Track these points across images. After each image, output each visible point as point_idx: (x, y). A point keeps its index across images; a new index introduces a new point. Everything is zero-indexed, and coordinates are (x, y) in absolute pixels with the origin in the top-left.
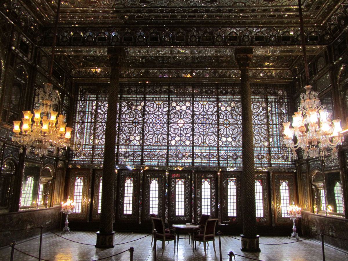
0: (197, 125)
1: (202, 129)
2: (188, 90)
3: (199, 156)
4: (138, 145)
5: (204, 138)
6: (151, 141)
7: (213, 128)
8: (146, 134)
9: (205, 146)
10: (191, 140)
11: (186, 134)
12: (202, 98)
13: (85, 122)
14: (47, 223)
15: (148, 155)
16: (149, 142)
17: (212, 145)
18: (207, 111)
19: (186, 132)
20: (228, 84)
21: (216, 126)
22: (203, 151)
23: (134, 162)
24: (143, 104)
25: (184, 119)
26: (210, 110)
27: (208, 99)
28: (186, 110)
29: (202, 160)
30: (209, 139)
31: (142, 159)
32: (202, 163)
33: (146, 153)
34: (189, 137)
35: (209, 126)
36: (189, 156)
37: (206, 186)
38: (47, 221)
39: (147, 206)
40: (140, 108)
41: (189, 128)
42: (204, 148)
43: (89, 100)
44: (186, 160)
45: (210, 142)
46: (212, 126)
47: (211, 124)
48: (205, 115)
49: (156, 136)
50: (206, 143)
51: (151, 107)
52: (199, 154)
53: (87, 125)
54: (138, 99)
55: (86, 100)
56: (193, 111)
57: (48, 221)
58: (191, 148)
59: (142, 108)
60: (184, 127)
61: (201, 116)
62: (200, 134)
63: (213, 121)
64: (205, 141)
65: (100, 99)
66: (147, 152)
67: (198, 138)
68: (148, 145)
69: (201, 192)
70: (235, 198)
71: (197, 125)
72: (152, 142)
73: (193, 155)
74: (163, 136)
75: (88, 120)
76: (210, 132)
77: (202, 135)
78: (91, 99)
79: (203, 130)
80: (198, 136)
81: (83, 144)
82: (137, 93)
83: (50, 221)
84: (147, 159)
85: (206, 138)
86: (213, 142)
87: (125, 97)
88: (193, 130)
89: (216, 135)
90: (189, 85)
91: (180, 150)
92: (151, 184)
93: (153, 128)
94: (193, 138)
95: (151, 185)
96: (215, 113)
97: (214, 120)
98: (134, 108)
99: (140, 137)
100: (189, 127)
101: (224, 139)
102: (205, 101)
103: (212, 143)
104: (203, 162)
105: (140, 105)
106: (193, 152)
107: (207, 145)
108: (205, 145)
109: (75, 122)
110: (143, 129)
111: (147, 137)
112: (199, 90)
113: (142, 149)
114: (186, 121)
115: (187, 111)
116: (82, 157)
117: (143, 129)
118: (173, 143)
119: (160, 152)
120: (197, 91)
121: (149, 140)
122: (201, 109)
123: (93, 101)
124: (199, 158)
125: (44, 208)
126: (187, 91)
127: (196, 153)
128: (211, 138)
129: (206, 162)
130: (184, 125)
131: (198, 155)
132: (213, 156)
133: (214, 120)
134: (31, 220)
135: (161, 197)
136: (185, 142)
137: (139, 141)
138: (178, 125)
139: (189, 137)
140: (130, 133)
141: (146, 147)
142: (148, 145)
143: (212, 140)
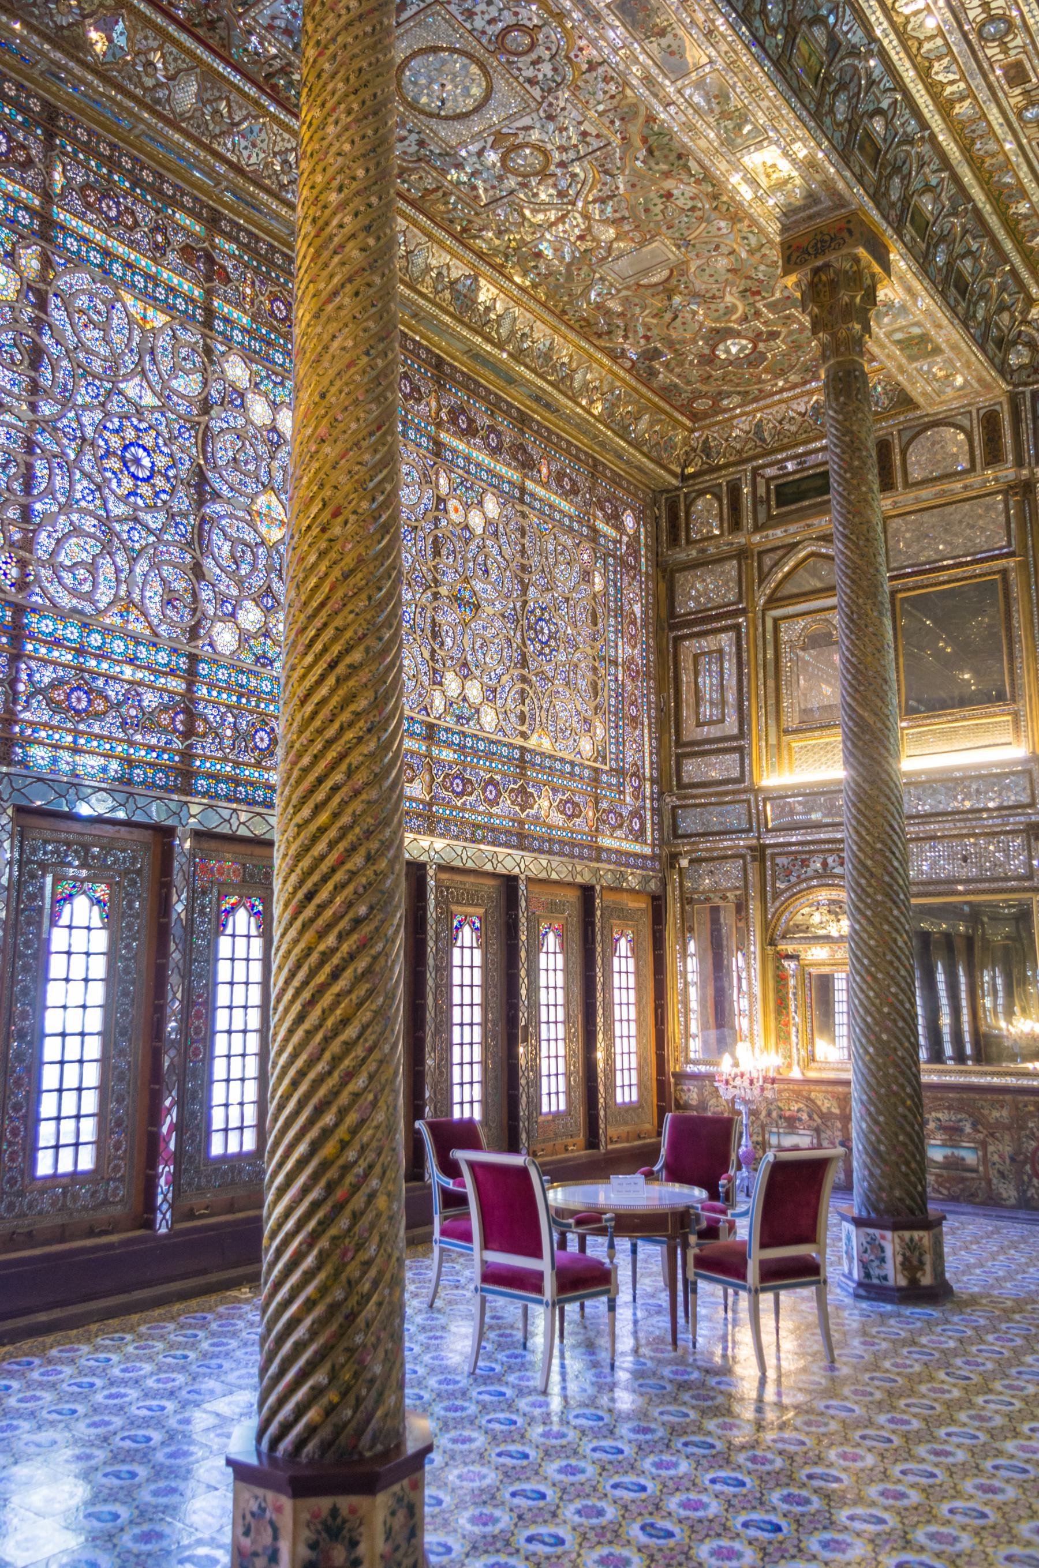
6: (86, 587)
8: (50, 518)
15: (59, 695)
16: (73, 592)
20: (480, 385)
33: (47, 675)
39: (17, 1107)
49: (121, 559)
66: (55, 663)
68: (62, 615)
74: (167, 571)
91: (259, 699)
92: (53, 923)
95: (59, 939)
101: (452, 683)
118: (225, 638)
119: (140, 683)
121: (70, 569)
135: (21, 1035)
138: (251, 525)
141: (47, 626)
142: (62, 615)
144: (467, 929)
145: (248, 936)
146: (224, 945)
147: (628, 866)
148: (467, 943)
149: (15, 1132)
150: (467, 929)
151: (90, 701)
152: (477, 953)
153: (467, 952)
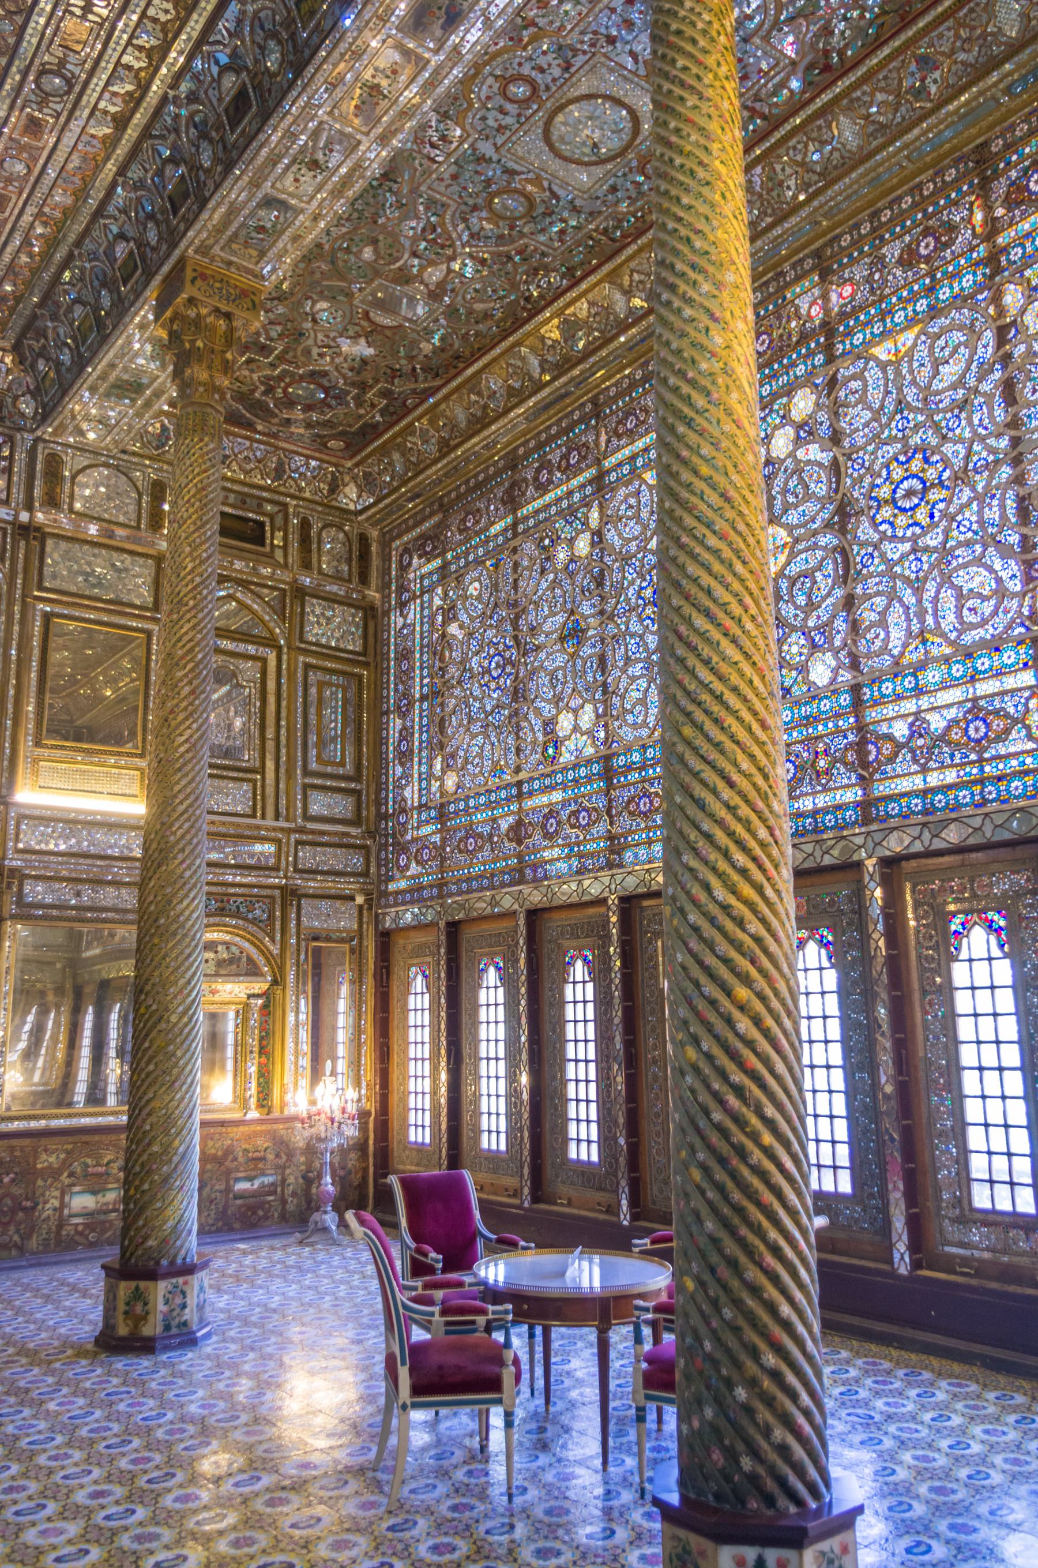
0: (865, 524)
1: (903, 539)
2: (797, 308)
3: (899, 747)
4: (589, 762)
5: (920, 601)
7: (980, 498)
9: (935, 660)
10: (837, 643)
11: (811, 606)
12: (883, 315)
13: (423, 698)
14: (242, 1186)
17: (986, 633)
18: (927, 393)
19: (809, 597)
21: (1006, 472)
22: (925, 702)
23: (581, 856)
24: (595, 515)
25: (793, 517)
26: (950, 372)
27: (922, 305)
28: (792, 455)
29: (924, 770)
30: (960, 596)
31: (611, 837)
32: (925, 792)
34: (830, 623)
35: (948, 501)
36: (835, 761)
37: (981, 970)
38: (237, 1180)
39: (657, 1115)
40: (583, 546)
41: (819, 568)
42: (932, 676)
43: (422, 593)
44: (825, 789)
45: (970, 618)
46: (973, 489)
47: (962, 477)
48: (917, 427)
50: (943, 635)
51: (630, 518)
52: (900, 730)
53: (422, 710)
54: (576, 497)
55: (414, 598)
56: (836, 438)
57: (250, 1179)
58: (845, 699)
59: (593, 544)
60: (794, 569)
61: (891, 450)
62: (894, 577)
63: (976, 447)
64: (930, 620)
65: (453, 568)
67: (883, 614)
69: (952, 1016)
70: (1017, 1063)
71: (865, 524)
72: (645, 724)
73: (860, 747)
75: (422, 686)
76: (960, 544)
77: (907, 581)
78: (426, 582)
79: (907, 546)
80: (880, 602)
81: (413, 808)
82: (569, 470)
83: (268, 1180)
84: (631, 832)
85: (935, 600)
86: (987, 608)
87: (526, 518)
88: (847, 574)
89: (1005, 552)
90: (798, 279)
93: (641, 637)
94: (855, 627)
96: (980, 380)
97: (982, 439)
98: (562, 556)
99: (596, 709)
100: (819, 553)
102: (911, 322)
103: (984, 622)
104: (934, 779)
105: (585, 524)
106: (861, 728)
107: (951, 643)
108: (935, 652)
109: (387, 713)
110: (602, 660)
111: (623, 697)
112: (859, 272)
113: (608, 774)
114: (798, 526)
115: (800, 454)
116: (414, 869)
117: (602, 660)
120: (847, 290)
122: (888, 393)
123: (431, 590)
124: (904, 763)
125: (237, 1116)
126: (789, 321)
127: (884, 729)
128: (976, 580)
129: (951, 776)
130: (792, 556)
131: (890, 737)
132: (998, 724)
133: (982, 439)
134: (100, 1169)
136: (803, 669)
137: (589, 733)
139: (830, 623)
140: (557, 700)
143: (984, 599)
144: (579, 964)
145: (821, 969)
146: (960, 973)
147: (470, 891)
148: (579, 977)
149: (658, 1135)
150: (579, 964)
151: (988, 726)
152: (590, 986)
153: (492, 991)
